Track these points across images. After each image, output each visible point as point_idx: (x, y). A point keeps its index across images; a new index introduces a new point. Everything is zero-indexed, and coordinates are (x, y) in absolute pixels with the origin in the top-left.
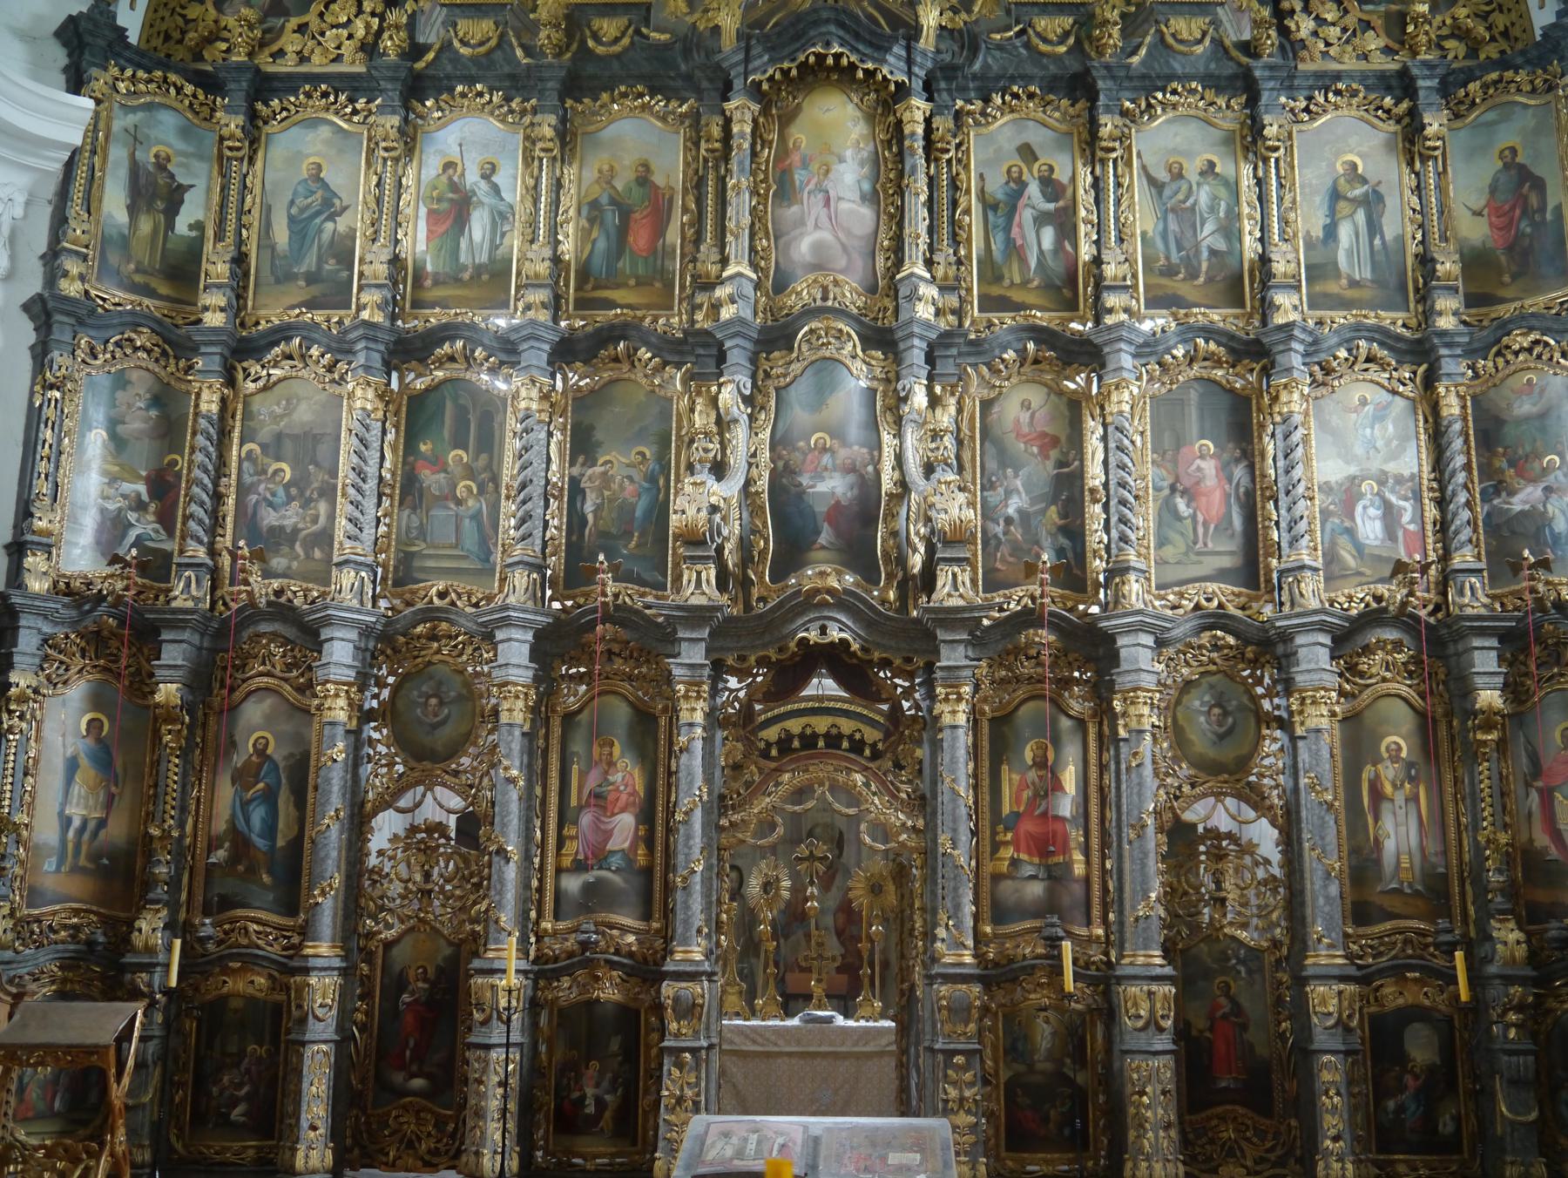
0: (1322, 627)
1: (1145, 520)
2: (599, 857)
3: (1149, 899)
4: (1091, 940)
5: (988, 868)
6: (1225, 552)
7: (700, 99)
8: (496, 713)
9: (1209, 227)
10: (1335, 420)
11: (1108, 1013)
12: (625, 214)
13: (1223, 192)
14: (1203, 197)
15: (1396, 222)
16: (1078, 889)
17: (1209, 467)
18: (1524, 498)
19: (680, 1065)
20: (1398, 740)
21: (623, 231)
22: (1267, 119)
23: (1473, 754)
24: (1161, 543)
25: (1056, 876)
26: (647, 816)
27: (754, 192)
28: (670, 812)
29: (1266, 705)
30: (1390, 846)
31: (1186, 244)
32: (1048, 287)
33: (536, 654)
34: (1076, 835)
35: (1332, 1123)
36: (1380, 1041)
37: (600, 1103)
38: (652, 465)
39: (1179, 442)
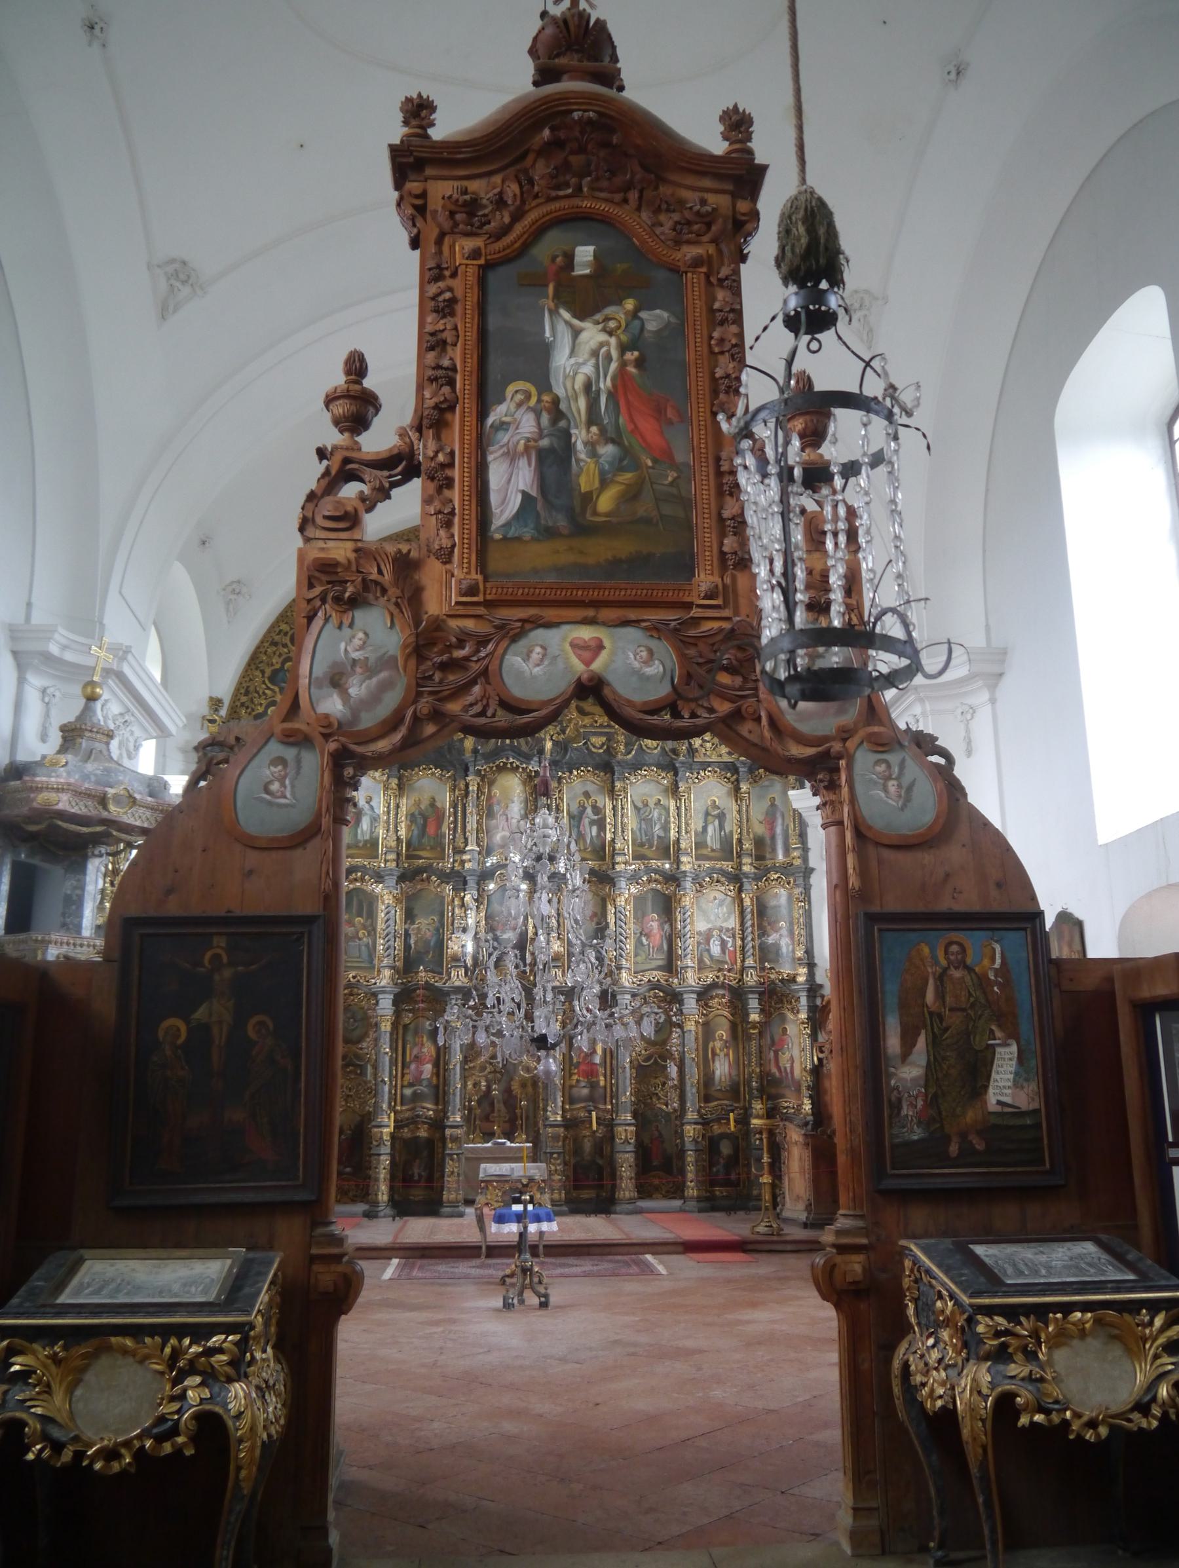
0: (693, 992)
1: (630, 946)
2: (417, 1081)
3: (627, 1096)
4: (607, 1111)
5: (567, 1084)
6: (660, 959)
7: (455, 771)
8: (376, 1024)
9: (657, 827)
10: (704, 906)
11: (611, 1137)
12: (425, 819)
13: (663, 812)
14: (656, 814)
15: (731, 825)
16: (601, 1091)
17: (655, 925)
18: (771, 940)
19: (452, 1160)
20: (723, 1032)
21: (425, 826)
22: (680, 784)
23: (749, 1038)
24: (636, 956)
25: (593, 1086)
26: (436, 1065)
27: (478, 814)
28: (446, 1063)
29: (674, 1019)
30: (718, 1073)
31: (649, 833)
32: (594, 851)
34: (601, 1070)
35: (690, 1176)
36: (710, 1146)
37: (420, 1176)
38: (437, 924)
39: (644, 915)
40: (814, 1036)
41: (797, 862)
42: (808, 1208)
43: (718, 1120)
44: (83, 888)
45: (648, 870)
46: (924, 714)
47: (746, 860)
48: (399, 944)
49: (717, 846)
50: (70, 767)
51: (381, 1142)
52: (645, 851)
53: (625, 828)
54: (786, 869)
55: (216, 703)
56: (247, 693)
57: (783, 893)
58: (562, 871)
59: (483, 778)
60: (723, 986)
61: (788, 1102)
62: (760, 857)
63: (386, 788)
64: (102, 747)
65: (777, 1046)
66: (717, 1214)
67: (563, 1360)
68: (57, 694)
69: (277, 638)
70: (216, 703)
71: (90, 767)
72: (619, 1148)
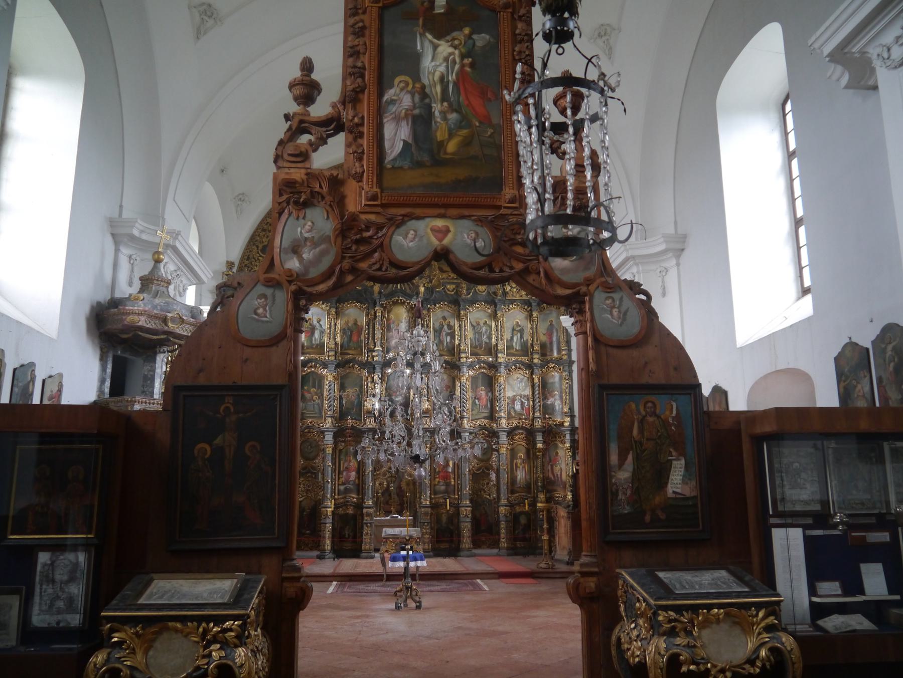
1: (469, 405)
3: (467, 490)
4: (455, 499)
11: (457, 513)
12: (351, 332)
14: (484, 330)
17: (483, 393)
18: (549, 402)
20: (522, 455)
23: (537, 457)
24: (472, 410)
25: (448, 484)
26: (358, 472)
28: (364, 472)
30: (519, 477)
31: (480, 340)
33: (334, 437)
34: (452, 476)
35: (503, 535)
36: (514, 519)
39: (477, 387)
40: (574, 457)
41: (565, 357)
42: (569, 553)
43: (519, 504)
44: (154, 371)
45: (479, 362)
46: (638, 272)
47: (536, 356)
48: (336, 403)
49: (519, 348)
50: (146, 301)
51: (326, 516)
52: (478, 350)
53: (466, 337)
54: (559, 361)
55: (230, 265)
56: (248, 259)
57: (557, 375)
58: (428, 361)
59: (384, 308)
60: (522, 428)
61: (559, 494)
62: (543, 354)
63: (329, 314)
64: (164, 289)
65: (553, 462)
66: (518, 557)
67: (428, 637)
68: (138, 259)
69: (265, 227)
70: (230, 265)
71: (157, 301)
72: (462, 519)
